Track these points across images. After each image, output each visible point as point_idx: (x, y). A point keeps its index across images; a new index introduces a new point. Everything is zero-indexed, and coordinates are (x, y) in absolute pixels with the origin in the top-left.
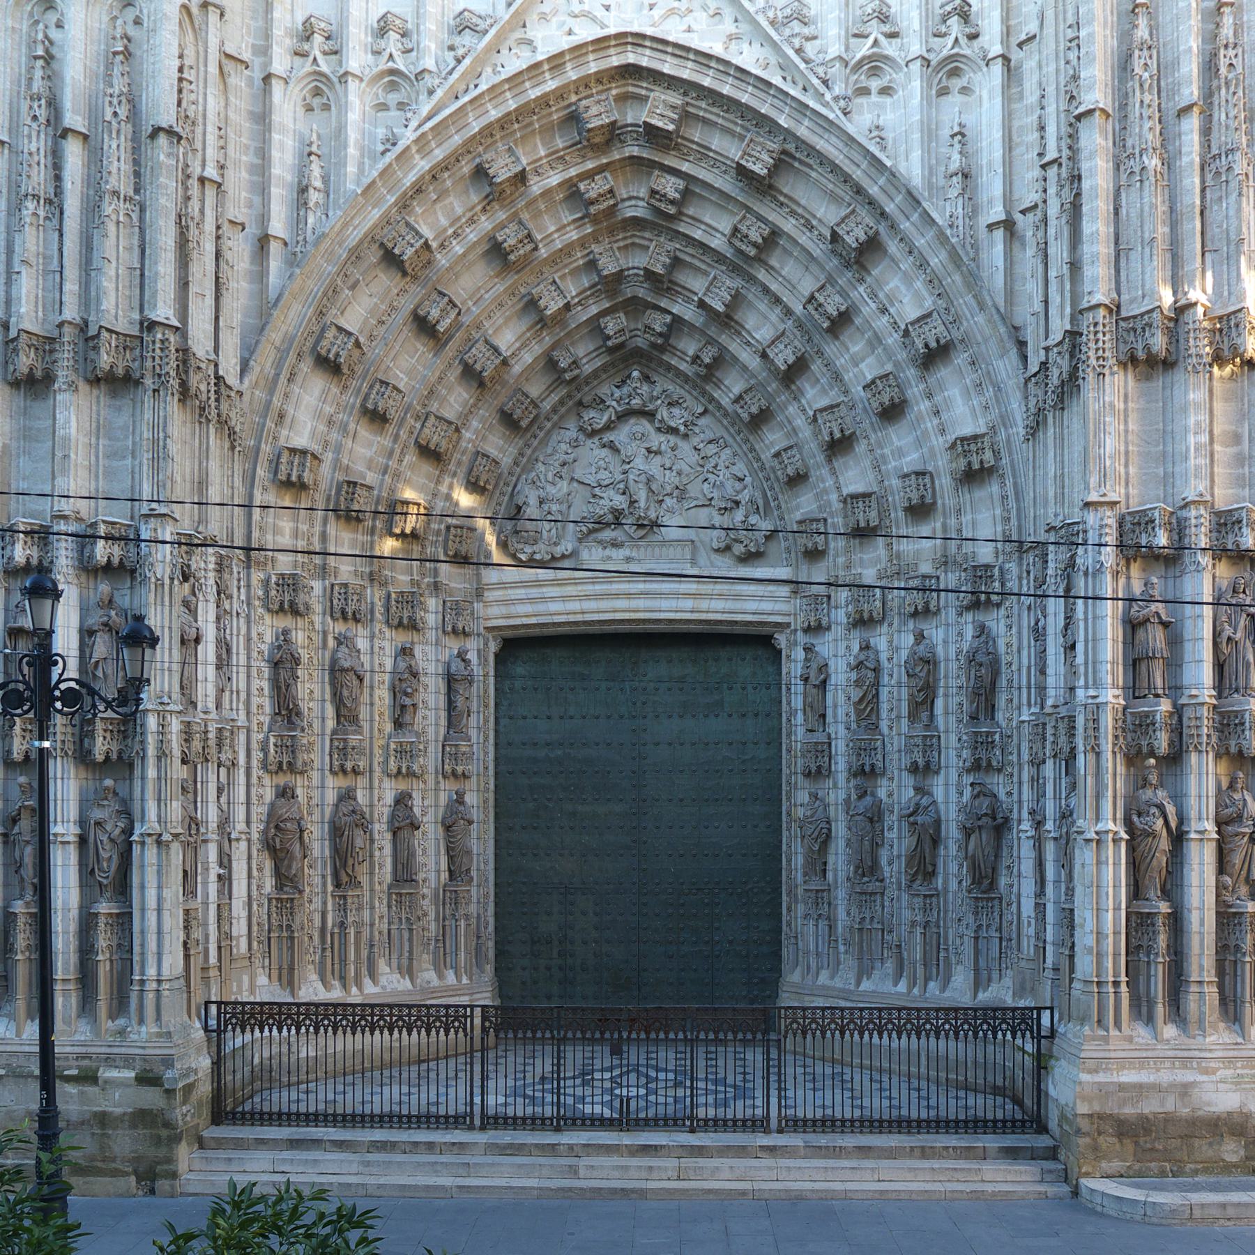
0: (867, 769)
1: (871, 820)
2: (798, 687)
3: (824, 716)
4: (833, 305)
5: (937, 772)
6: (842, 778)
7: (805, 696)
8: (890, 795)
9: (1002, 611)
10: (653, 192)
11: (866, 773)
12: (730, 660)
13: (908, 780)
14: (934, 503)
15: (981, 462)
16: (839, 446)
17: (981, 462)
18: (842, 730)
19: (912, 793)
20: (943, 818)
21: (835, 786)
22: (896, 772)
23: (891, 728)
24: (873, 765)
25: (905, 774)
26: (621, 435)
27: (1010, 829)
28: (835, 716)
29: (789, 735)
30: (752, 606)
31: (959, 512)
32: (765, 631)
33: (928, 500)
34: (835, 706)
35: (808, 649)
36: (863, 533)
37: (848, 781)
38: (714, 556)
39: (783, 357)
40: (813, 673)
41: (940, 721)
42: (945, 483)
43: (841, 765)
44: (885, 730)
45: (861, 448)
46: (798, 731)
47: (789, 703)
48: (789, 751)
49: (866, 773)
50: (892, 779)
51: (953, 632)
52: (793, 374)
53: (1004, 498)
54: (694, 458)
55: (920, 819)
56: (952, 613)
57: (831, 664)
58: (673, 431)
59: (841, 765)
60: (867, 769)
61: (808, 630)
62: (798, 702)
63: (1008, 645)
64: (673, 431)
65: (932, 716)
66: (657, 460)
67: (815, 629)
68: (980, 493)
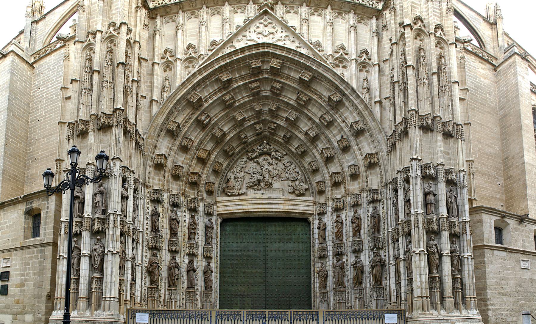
0: (340, 252)
1: (341, 268)
3: (325, 239)
5: (362, 252)
6: (331, 258)
7: (319, 234)
8: (347, 261)
9: (381, 203)
11: (339, 255)
12: (294, 226)
13: (353, 255)
14: (359, 174)
15: (374, 161)
16: (329, 160)
17: (374, 161)
18: (331, 243)
19: (354, 258)
21: (329, 260)
22: (349, 253)
23: (347, 240)
24: (341, 252)
25: (352, 253)
28: (329, 238)
29: (313, 247)
31: (367, 176)
32: (305, 216)
33: (358, 173)
34: (329, 236)
36: (336, 185)
37: (333, 258)
41: (362, 237)
42: (362, 168)
43: (330, 254)
44: (345, 241)
45: (336, 161)
47: (313, 237)
48: (314, 252)
49: (339, 255)
50: (347, 256)
51: (366, 210)
52: (314, 140)
55: (357, 265)
57: (327, 224)
59: (330, 254)
60: (340, 252)
62: (316, 236)
63: (383, 212)
65: (360, 235)
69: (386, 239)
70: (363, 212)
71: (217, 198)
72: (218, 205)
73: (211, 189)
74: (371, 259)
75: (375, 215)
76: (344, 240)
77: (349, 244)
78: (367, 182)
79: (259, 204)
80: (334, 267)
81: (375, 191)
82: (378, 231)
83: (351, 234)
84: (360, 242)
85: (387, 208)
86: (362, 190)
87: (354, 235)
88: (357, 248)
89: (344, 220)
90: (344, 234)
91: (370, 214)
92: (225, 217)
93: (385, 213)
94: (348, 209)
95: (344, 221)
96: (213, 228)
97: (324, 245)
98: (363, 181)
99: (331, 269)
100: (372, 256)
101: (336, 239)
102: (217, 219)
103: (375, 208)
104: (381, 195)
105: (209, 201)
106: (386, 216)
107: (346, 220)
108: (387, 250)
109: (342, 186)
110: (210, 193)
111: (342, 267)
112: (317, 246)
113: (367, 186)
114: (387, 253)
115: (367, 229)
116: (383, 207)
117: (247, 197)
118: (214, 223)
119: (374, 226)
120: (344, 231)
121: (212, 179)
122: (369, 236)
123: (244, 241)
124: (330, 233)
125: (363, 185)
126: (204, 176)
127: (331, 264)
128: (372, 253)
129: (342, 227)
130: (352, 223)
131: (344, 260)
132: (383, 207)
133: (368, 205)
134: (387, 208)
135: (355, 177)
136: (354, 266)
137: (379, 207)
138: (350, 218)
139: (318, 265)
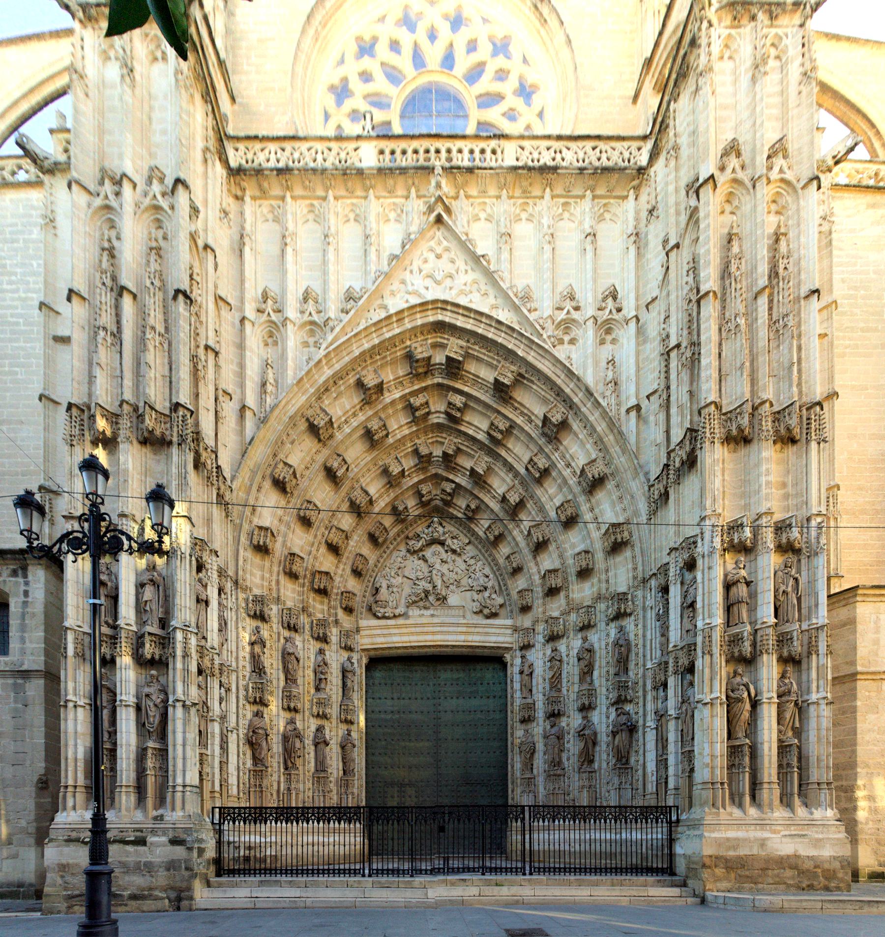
2: (517, 678)
3: (531, 690)
4: (542, 463)
5: (594, 709)
6: (541, 721)
7: (521, 682)
9: (633, 618)
10: (450, 403)
11: (554, 715)
16: (540, 547)
18: (541, 697)
19: (580, 721)
20: (598, 730)
29: (512, 704)
30: (493, 639)
31: (607, 571)
35: (523, 657)
36: (552, 592)
38: (475, 616)
39: (513, 498)
40: (526, 669)
43: (540, 714)
46: (517, 699)
49: (554, 715)
51: (603, 634)
53: (634, 557)
54: (463, 566)
56: (603, 624)
58: (454, 552)
59: (540, 714)
61: (522, 648)
62: (517, 686)
64: (454, 552)
65: (592, 681)
66: (446, 566)
67: (526, 647)
68: (619, 559)
70: (600, 639)
76: (564, 691)
77: (573, 696)
78: (607, 581)
79: (427, 633)
80: (546, 737)
81: (622, 597)
82: (626, 670)
83: (576, 679)
84: (591, 693)
85: (644, 627)
86: (599, 598)
87: (582, 680)
88: (587, 703)
89: (564, 655)
90: (564, 681)
91: (611, 640)
93: (640, 636)
94: (571, 635)
95: (565, 658)
97: (529, 701)
98: (600, 581)
99: (541, 740)
100: (613, 715)
101: (551, 689)
103: (621, 629)
107: (568, 656)
109: (562, 594)
111: (560, 737)
112: (518, 702)
113: (607, 589)
115: (606, 669)
116: (637, 625)
117: (408, 622)
119: (619, 662)
120: (564, 675)
121: (352, 584)
122: (608, 680)
124: (541, 680)
125: (600, 589)
127: (541, 731)
128: (612, 710)
129: (560, 668)
130: (579, 660)
131: (564, 724)
132: (637, 625)
133: (608, 625)
134: (644, 627)
135: (584, 573)
136: (580, 734)
138: (576, 651)
139: (519, 733)
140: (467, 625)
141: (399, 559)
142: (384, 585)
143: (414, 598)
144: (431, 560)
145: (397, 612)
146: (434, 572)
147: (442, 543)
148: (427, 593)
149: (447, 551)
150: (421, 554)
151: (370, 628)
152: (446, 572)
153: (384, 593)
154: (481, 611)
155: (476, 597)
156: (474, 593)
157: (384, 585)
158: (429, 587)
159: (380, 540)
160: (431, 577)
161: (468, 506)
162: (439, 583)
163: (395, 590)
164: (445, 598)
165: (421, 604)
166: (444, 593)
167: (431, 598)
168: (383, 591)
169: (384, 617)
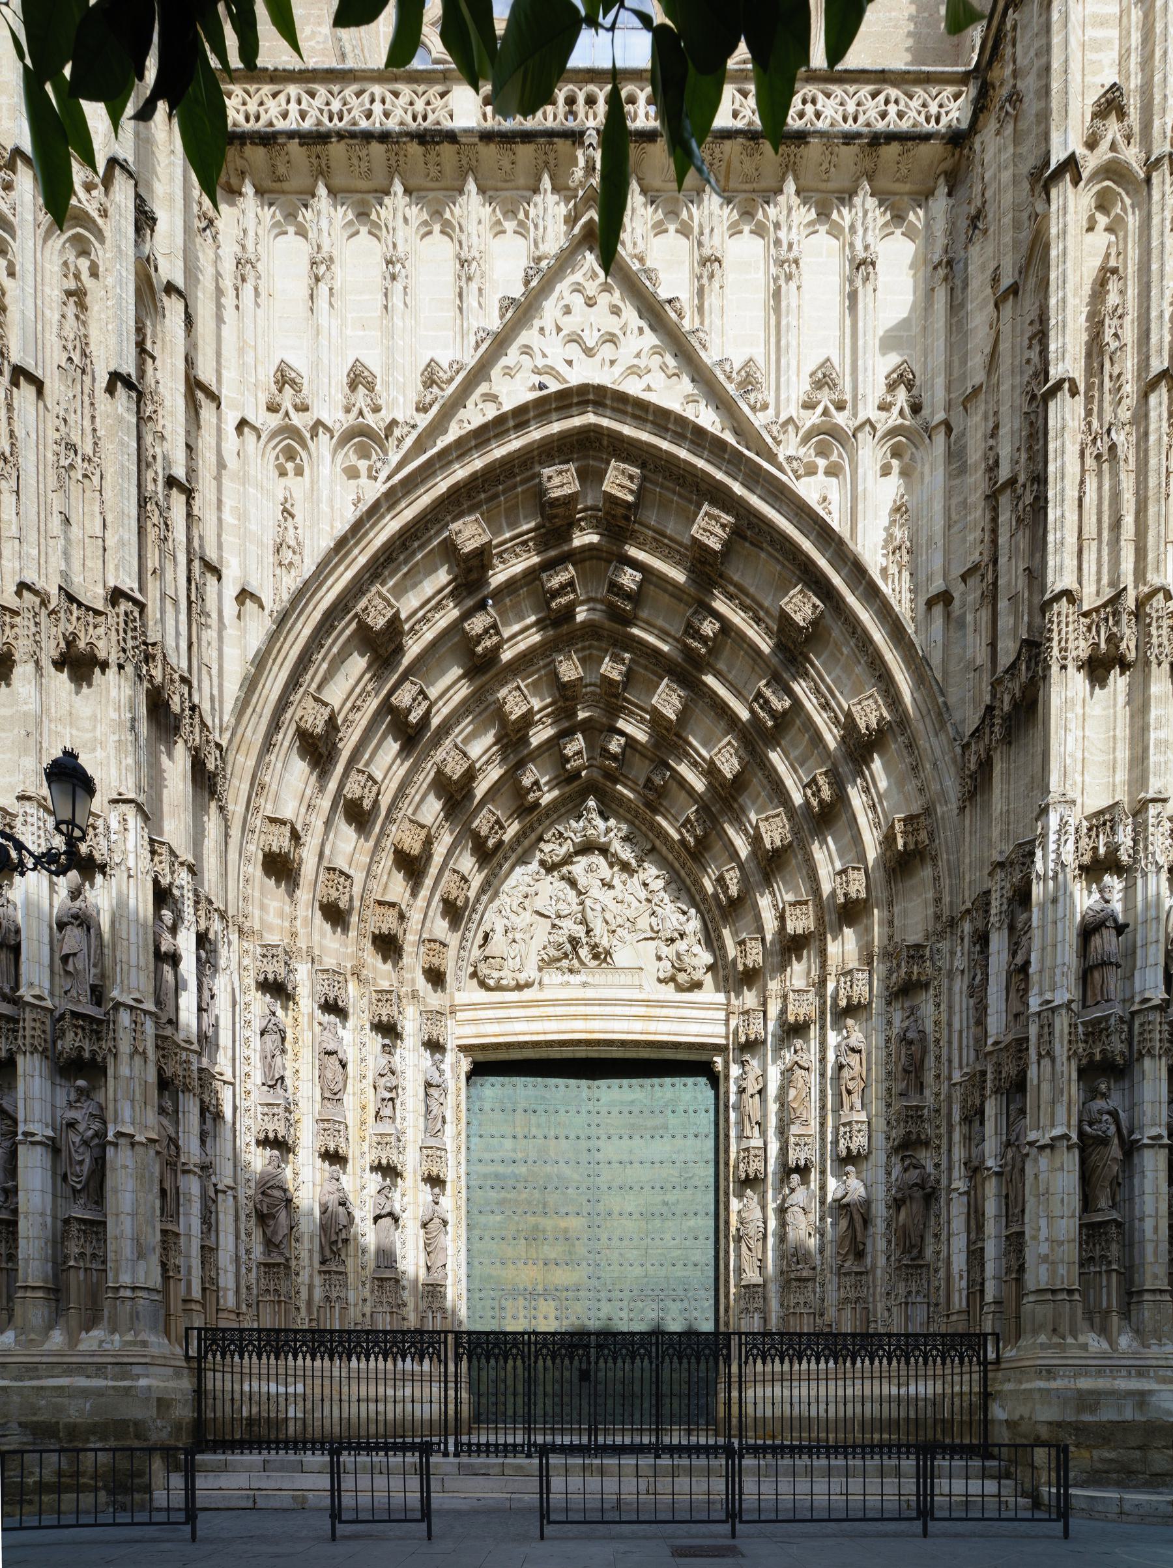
26: (579, 867)
27: (937, 1199)
66: (611, 893)
69: (944, 1111)
71: (457, 995)
72: (460, 1016)
73: (436, 961)
74: (894, 1177)
75: (910, 1035)
82: (921, 1087)
91: (895, 1031)
92: (481, 1057)
93: (944, 1025)
96: (445, 1091)
100: (896, 1171)
102: (459, 1061)
104: (933, 964)
105: (435, 1000)
106: (945, 1033)
108: (944, 1148)
110: (436, 977)
114: (945, 1158)
116: (938, 1005)
118: (448, 1075)
123: (534, 1131)
126: (415, 917)
132: (938, 1005)
137: (923, 1006)
140: (647, 1003)
141: (528, 879)
142: (500, 929)
143: (553, 953)
144: (582, 882)
145: (522, 978)
146: (588, 902)
147: (604, 850)
148: (574, 942)
149: (611, 866)
150: (564, 870)
151: (475, 1006)
152: (612, 905)
153: (498, 944)
154: (673, 979)
155: (666, 951)
156: (662, 945)
157: (500, 929)
158: (579, 931)
159: (491, 843)
160: (583, 912)
161: (649, 780)
162: (598, 927)
163: (518, 936)
164: (608, 953)
165: (565, 963)
166: (605, 942)
167: (584, 952)
168: (498, 938)
169: (499, 988)
